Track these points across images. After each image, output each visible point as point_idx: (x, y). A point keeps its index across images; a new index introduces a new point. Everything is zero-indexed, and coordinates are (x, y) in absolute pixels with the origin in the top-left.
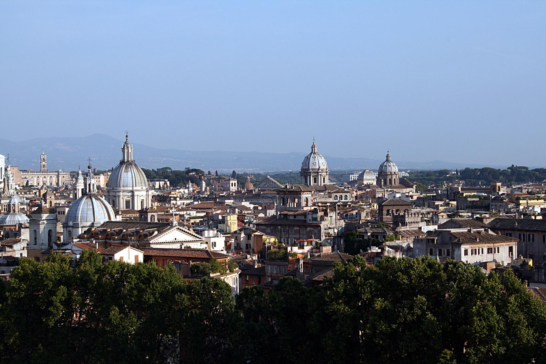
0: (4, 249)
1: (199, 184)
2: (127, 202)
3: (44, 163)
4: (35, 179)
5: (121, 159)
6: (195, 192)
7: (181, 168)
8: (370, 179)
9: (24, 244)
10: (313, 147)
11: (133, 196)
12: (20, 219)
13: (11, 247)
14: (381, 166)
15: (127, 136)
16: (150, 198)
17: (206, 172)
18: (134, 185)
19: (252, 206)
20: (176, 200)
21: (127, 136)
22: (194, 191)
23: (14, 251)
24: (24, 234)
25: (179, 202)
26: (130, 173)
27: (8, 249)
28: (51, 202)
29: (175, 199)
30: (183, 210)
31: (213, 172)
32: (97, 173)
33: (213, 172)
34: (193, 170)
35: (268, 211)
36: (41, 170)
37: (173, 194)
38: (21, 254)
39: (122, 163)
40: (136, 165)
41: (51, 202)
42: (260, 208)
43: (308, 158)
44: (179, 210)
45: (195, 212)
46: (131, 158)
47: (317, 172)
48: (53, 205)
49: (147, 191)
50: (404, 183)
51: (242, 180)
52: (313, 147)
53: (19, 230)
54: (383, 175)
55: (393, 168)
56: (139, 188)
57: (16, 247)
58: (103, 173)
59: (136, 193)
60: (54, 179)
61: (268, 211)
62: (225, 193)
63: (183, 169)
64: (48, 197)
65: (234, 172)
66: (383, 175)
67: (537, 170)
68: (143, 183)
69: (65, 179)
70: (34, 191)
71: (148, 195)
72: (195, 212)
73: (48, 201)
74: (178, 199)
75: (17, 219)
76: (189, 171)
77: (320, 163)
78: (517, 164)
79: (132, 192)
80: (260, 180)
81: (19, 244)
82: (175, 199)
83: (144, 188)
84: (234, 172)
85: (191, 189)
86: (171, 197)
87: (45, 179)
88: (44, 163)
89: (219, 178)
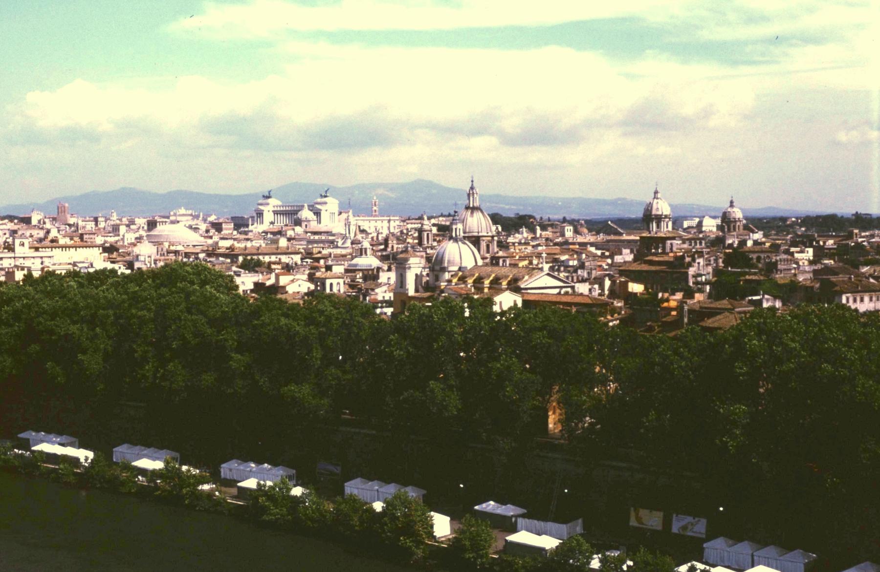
1: (534, 231)
3: (375, 208)
10: (656, 192)
14: (725, 214)
17: (538, 217)
28: (393, 247)
35: (616, 257)
42: (607, 254)
46: (477, 204)
48: (395, 250)
52: (656, 192)
54: (727, 223)
55: (737, 213)
61: (616, 257)
63: (512, 216)
64: (390, 242)
73: (390, 246)
88: (375, 208)
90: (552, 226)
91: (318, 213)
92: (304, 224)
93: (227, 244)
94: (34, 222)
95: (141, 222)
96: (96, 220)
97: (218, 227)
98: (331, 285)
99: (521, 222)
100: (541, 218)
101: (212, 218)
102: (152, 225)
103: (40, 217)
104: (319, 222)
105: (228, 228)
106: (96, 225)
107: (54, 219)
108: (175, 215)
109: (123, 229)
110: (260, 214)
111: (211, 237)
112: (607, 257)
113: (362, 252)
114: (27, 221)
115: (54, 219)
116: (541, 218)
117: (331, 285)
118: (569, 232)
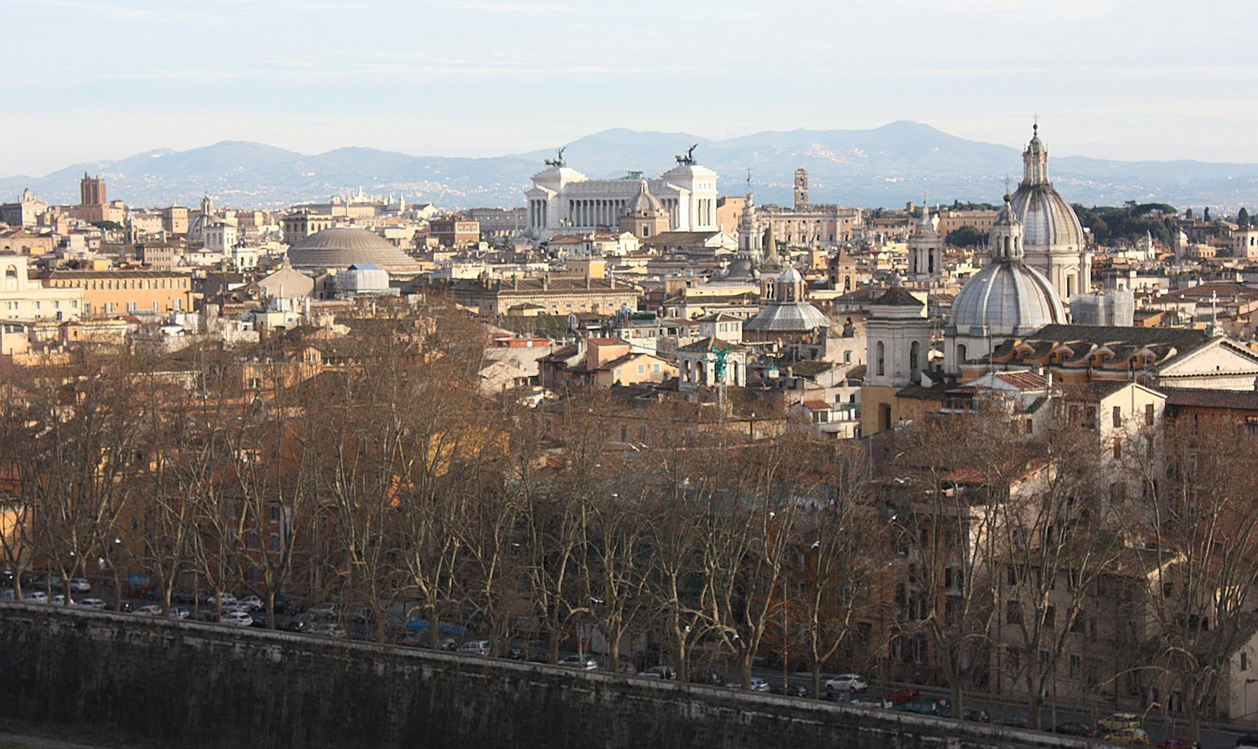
0: (799, 384)
4: (783, 224)
5: (1021, 179)
6: (1161, 257)
7: (1117, 202)
9: (839, 375)
12: (805, 317)
13: (812, 378)
15: (1035, 127)
16: (1088, 271)
18: (1052, 241)
20: (1128, 278)
21: (1035, 127)
22: (1157, 255)
23: (822, 388)
24: (832, 350)
26: (1041, 213)
27: (807, 384)
28: (848, 280)
29: (1125, 274)
38: (838, 397)
39: (1024, 188)
40: (1055, 193)
41: (848, 280)
44: (1156, 301)
45: (1193, 305)
49: (1082, 256)
53: (821, 342)
56: (1064, 248)
57: (822, 379)
59: (1055, 260)
62: (1236, 261)
63: (1118, 203)
64: (841, 268)
65: (1243, 209)
68: (1073, 238)
70: (793, 254)
71: (1082, 265)
72: (1193, 305)
73: (842, 277)
74: (1133, 274)
75: (798, 317)
81: (828, 373)
82: (1125, 274)
83: (1075, 248)
84: (1243, 209)
85: (1152, 251)
86: (1115, 270)
87: (803, 227)
91: (671, 203)
93: (469, 272)
96: (166, 216)
97: (443, 229)
100: (1189, 213)
104: (674, 220)
108: (343, 204)
113: (783, 295)
116: (1189, 213)
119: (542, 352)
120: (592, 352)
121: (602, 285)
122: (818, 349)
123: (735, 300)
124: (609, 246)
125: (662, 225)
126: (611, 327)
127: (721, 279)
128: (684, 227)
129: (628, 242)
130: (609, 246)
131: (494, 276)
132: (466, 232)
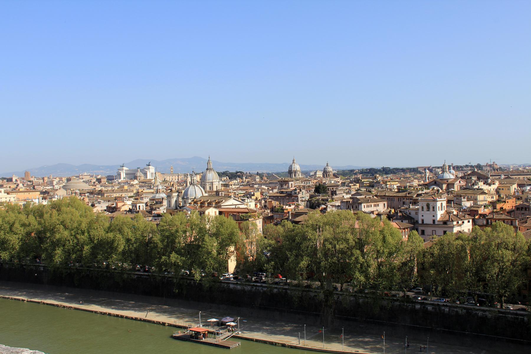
1: (242, 179)
2: (210, 187)
8: (320, 174)
10: (294, 161)
11: (212, 184)
14: (325, 169)
17: (245, 173)
19: (266, 188)
25: (233, 187)
27: (157, 209)
29: (231, 185)
30: (235, 190)
31: (248, 172)
32: (196, 174)
33: (248, 172)
34: (239, 172)
36: (172, 174)
37: (230, 183)
39: (207, 169)
43: (291, 166)
46: (211, 167)
47: (295, 172)
50: (335, 176)
51: (261, 176)
52: (294, 161)
54: (325, 173)
55: (330, 169)
58: (198, 174)
60: (177, 177)
63: (234, 171)
66: (325, 173)
67: (394, 169)
69: (181, 177)
76: (237, 172)
77: (297, 167)
78: (385, 166)
79: (212, 182)
80: (269, 176)
82: (231, 185)
89: (251, 176)
90: (251, 176)
91: (145, 174)
92: (138, 178)
94: (14, 180)
95: (64, 179)
96: (43, 179)
97: (99, 180)
98: (139, 206)
99: (233, 176)
101: (99, 177)
102: (69, 180)
103: (16, 178)
105: (104, 181)
106: (44, 181)
107: (23, 179)
108: (82, 175)
109: (55, 183)
110: (119, 175)
111: (96, 186)
112: (270, 190)
114: (10, 180)
115: (23, 179)
117: (139, 206)
118: (258, 179)
119: (107, 205)
120: (117, 204)
121: (127, 191)
122: (161, 203)
123: (153, 193)
124: (132, 182)
125: (142, 178)
126: (121, 199)
127: (151, 188)
128: (148, 178)
129: (136, 182)
130: (132, 182)
131: (104, 189)
132: (104, 181)
